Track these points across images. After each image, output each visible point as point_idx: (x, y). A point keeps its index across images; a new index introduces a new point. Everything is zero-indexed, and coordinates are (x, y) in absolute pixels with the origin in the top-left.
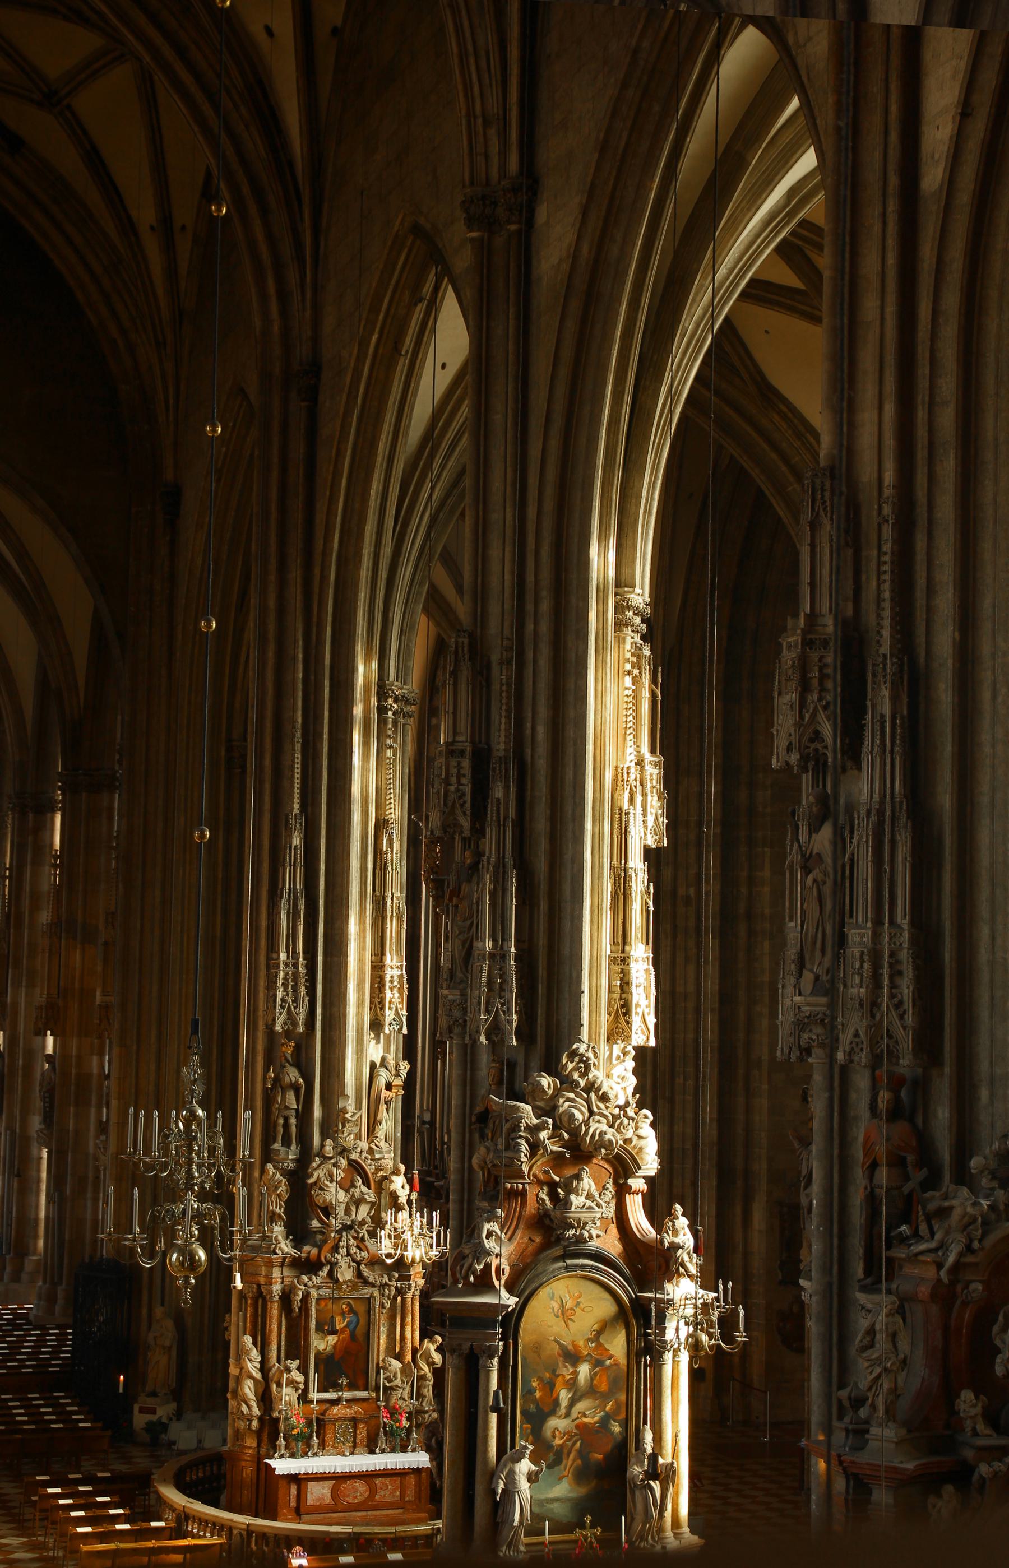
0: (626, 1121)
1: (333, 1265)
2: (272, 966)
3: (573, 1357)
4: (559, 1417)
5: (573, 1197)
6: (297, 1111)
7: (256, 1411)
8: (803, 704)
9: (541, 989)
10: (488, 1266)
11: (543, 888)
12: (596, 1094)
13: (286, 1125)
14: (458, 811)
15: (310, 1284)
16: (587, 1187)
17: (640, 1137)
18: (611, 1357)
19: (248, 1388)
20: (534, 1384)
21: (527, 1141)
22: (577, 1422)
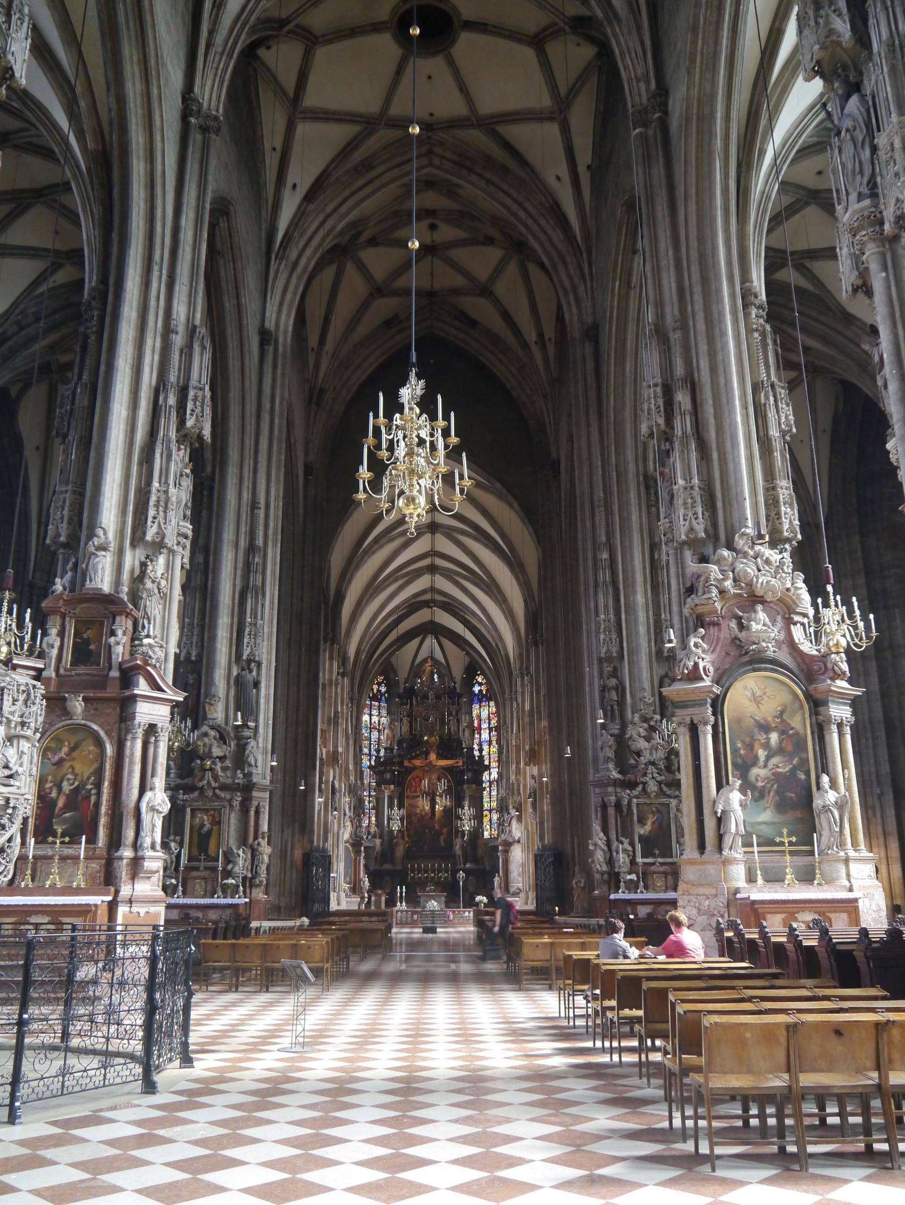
0: (784, 575)
1: (644, 784)
2: (598, 624)
3: (766, 728)
4: (760, 767)
5: (753, 623)
6: (617, 701)
7: (605, 868)
8: (817, 17)
9: (719, 504)
10: (696, 665)
12: (762, 559)
13: (612, 710)
17: (797, 588)
18: (792, 729)
19: (599, 856)
20: (739, 745)
21: (717, 587)
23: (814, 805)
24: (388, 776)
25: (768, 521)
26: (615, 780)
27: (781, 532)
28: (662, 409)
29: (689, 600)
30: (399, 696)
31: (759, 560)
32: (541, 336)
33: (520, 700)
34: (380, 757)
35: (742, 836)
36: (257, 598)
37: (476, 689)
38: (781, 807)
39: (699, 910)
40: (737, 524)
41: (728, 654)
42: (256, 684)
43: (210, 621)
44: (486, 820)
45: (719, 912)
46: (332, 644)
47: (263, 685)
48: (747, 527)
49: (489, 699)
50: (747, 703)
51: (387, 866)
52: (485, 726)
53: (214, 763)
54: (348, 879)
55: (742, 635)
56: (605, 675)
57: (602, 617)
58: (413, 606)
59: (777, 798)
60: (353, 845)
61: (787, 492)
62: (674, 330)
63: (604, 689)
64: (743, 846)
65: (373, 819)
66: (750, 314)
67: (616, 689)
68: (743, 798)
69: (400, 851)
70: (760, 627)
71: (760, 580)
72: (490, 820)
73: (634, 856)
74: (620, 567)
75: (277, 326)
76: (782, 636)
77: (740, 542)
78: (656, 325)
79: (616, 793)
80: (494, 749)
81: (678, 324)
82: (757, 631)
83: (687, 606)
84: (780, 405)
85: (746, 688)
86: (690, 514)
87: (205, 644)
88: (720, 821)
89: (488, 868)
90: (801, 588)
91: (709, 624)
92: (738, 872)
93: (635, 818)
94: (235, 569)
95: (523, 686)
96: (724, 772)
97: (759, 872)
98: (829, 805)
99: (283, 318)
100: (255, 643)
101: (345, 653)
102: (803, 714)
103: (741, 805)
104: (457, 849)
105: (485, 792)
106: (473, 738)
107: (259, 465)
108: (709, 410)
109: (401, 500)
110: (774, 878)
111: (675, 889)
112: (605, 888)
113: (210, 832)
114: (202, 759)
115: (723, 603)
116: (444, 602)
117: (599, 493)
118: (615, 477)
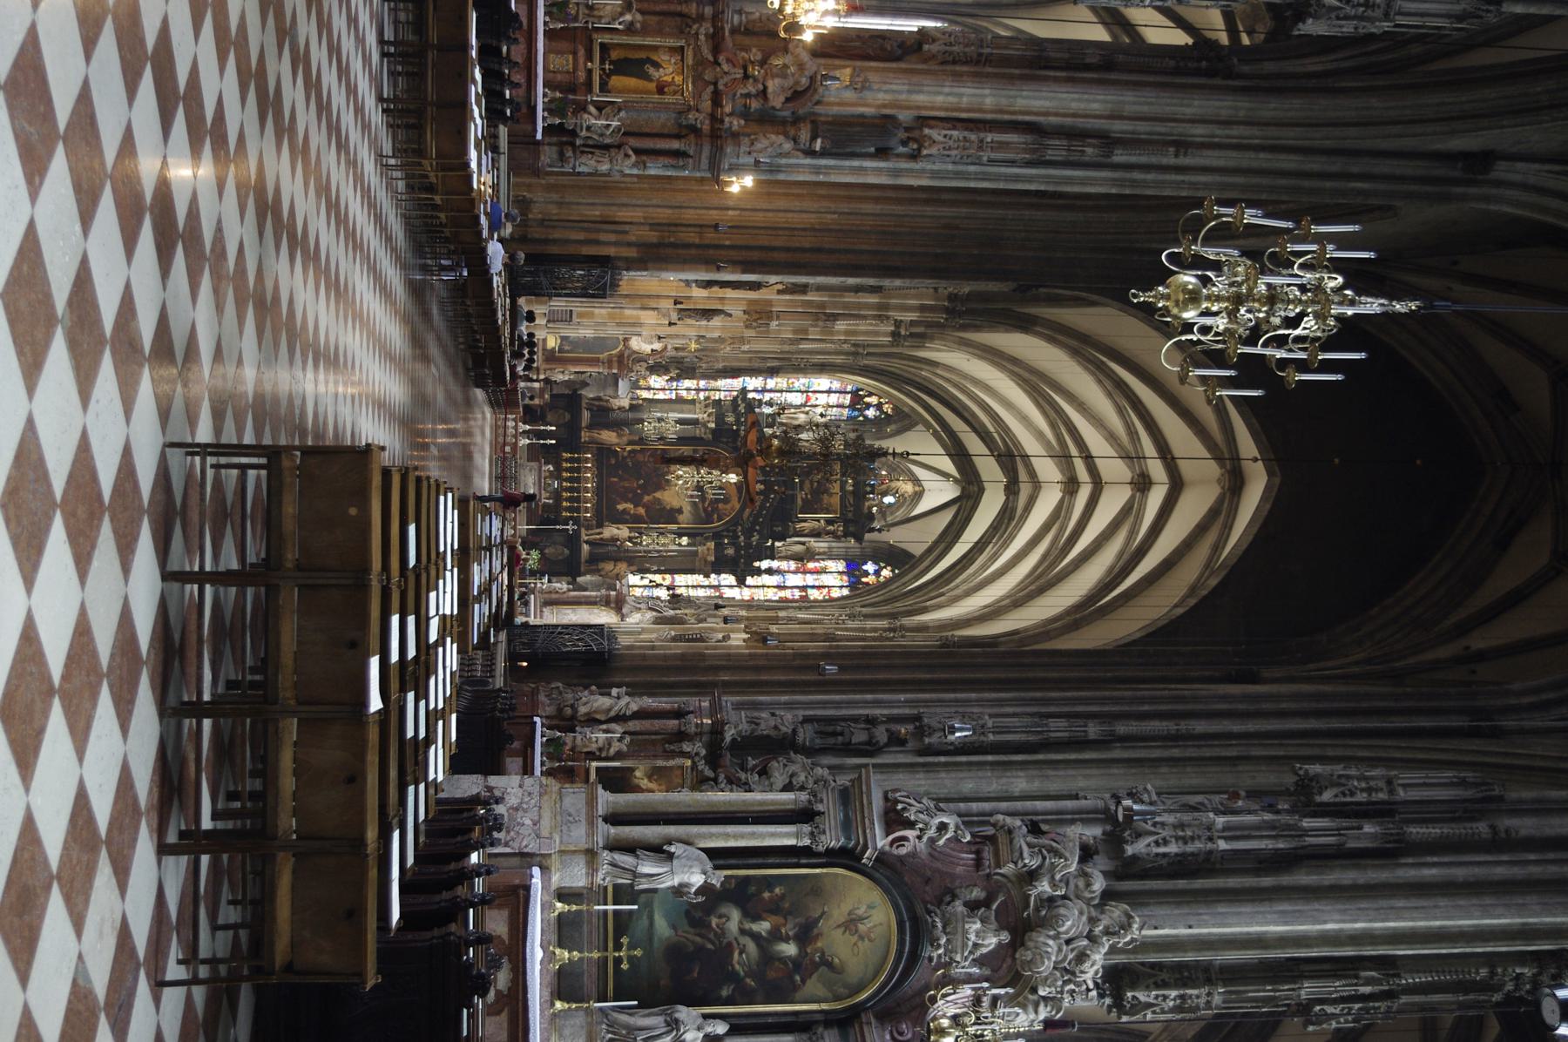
0: (1060, 983)
3: (805, 935)
4: (741, 922)
7: (583, 710)
9: (1181, 884)
10: (911, 825)
11: (1286, 880)
12: (1085, 947)
13: (835, 734)
14: (1335, 791)
15: (697, 759)
16: (986, 942)
18: (803, 981)
19: (602, 702)
20: (777, 890)
21: (1040, 867)
22: (735, 945)
23: (680, 1007)
24: (730, 419)
25: (1153, 966)
26: (721, 733)
27: (1133, 988)
28: (1348, 799)
29: (1018, 823)
30: (860, 438)
31: (1085, 942)
32: (1481, 656)
33: (850, 624)
34: (759, 407)
35: (632, 886)
36: (1025, 151)
37: (870, 567)
38: (675, 952)
39: (517, 809)
40: (1146, 912)
41: (928, 881)
42: (882, 153)
43: (988, 75)
44: (658, 578)
45: (513, 839)
46: (947, 310)
47: (882, 164)
48: (1141, 928)
49: (853, 586)
50: (846, 907)
51: (586, 415)
52: (810, 580)
53: (756, 80)
54: (567, 348)
55: (959, 907)
56: (895, 727)
57: (990, 724)
58: (1010, 458)
59: (692, 949)
60: (621, 356)
61: (1202, 1001)
62: (1492, 827)
63: (871, 721)
64: (616, 887)
65: (661, 396)
66: (1523, 964)
67: (869, 743)
68: (693, 890)
69: (608, 436)
70: (973, 937)
71: (1051, 942)
72: (658, 586)
73: (600, 759)
74: (1073, 756)
75: (1499, 183)
76: (957, 971)
77: (1116, 911)
78: (1501, 799)
79: (701, 734)
80: (773, 595)
81: (1503, 835)
82: (965, 932)
83: (1009, 820)
84: (1357, 1006)
85: (870, 907)
86: (1164, 833)
87: (949, 68)
88: (658, 850)
89: (580, 579)
90: (1036, 1012)
91: (978, 853)
92: (575, 876)
93: (660, 763)
94: (1074, 115)
95: (875, 630)
96: (733, 862)
97: (574, 908)
98: (678, 1030)
99: (1509, 193)
100: (950, 149)
101: (932, 339)
102: (825, 1001)
103: (682, 885)
104: (610, 531)
105: (698, 579)
106: (787, 558)
107: (1252, 155)
108: (1348, 876)
109: (1193, 280)
110: (564, 931)
111: (548, 773)
112: (550, 710)
113: (648, 78)
114: (763, 63)
115: (1014, 879)
116: (1014, 510)
117: (1200, 727)
118: (1228, 754)
